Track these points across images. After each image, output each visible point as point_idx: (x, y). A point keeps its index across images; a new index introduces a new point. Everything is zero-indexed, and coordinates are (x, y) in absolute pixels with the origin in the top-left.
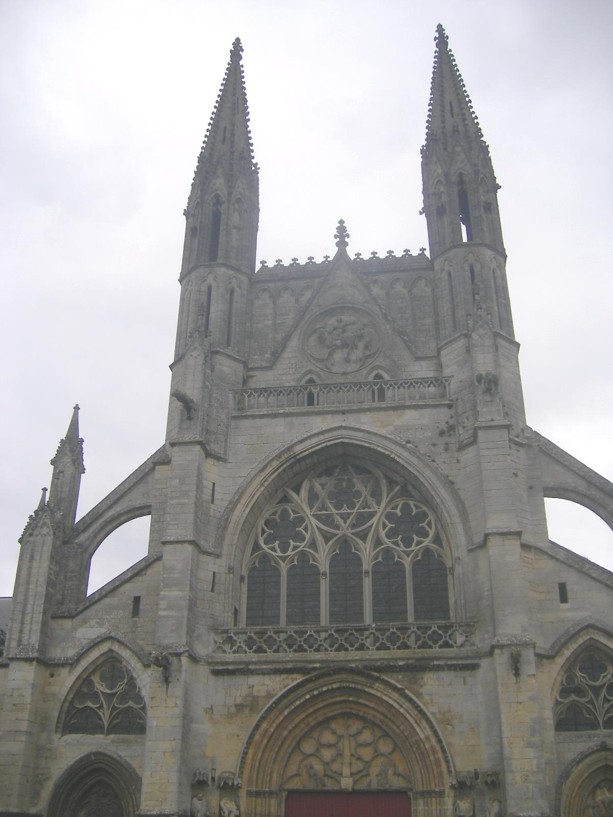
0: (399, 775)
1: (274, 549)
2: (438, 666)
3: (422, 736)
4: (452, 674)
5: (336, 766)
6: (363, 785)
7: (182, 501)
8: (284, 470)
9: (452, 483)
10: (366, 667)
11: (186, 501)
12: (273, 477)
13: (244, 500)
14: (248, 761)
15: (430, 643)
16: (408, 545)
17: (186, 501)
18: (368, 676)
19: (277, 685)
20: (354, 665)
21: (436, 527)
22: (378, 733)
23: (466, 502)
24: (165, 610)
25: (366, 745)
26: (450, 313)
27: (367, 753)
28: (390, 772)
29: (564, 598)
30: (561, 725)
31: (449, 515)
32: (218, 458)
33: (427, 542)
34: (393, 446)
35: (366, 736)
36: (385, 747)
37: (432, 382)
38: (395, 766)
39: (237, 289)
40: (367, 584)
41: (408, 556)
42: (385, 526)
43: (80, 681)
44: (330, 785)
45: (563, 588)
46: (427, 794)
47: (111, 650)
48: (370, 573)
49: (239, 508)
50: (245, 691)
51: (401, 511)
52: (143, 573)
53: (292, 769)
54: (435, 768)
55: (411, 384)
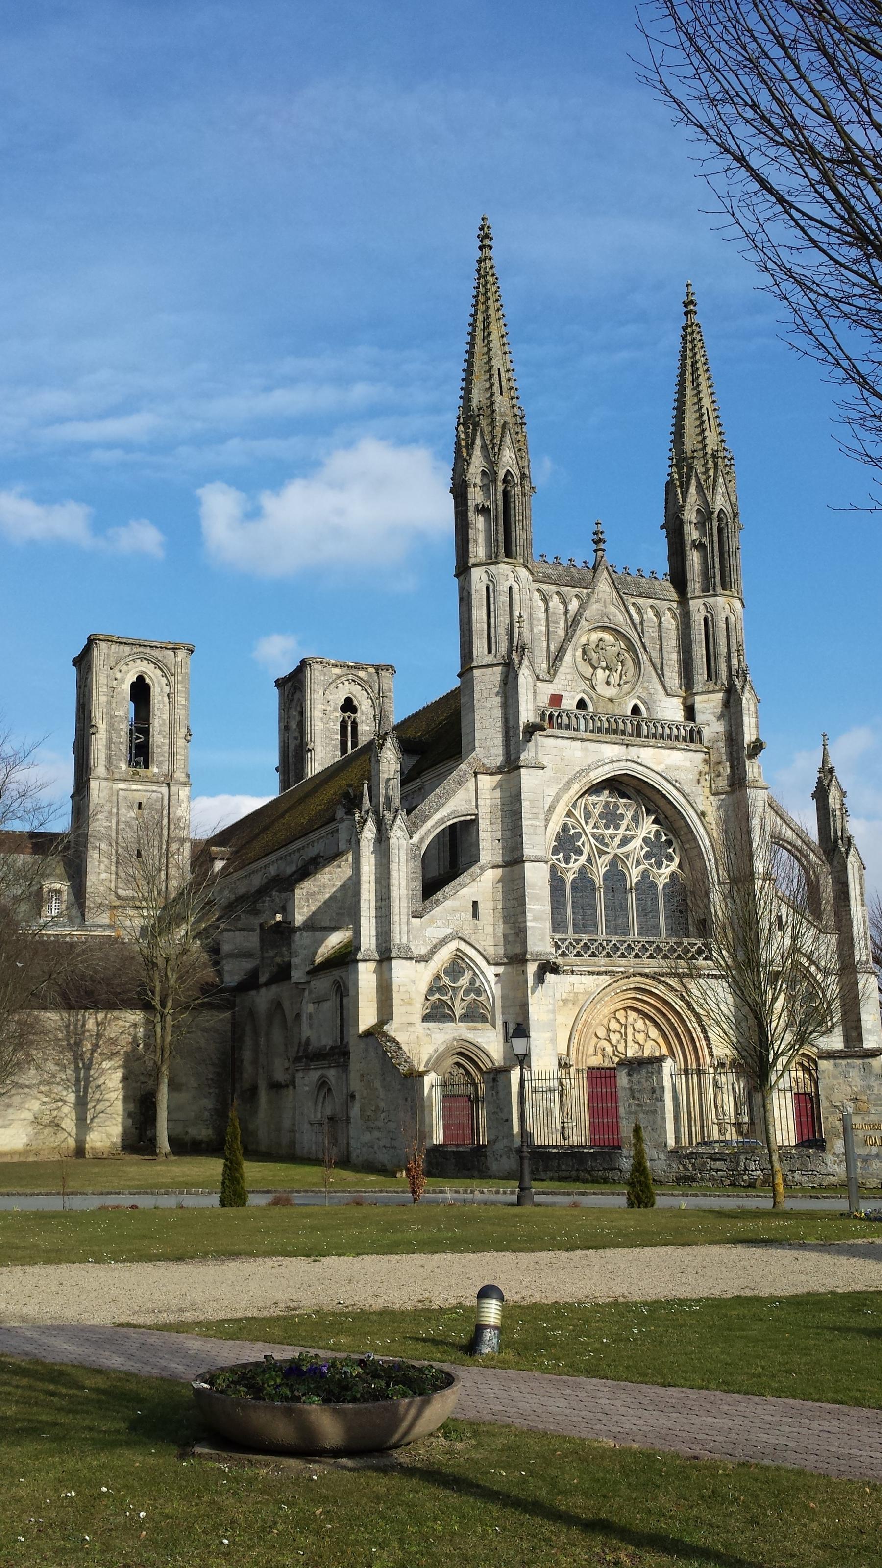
7: (534, 822)
10: (655, 973)
11: (538, 823)
42: (642, 848)
47: (458, 949)
50: (569, 989)
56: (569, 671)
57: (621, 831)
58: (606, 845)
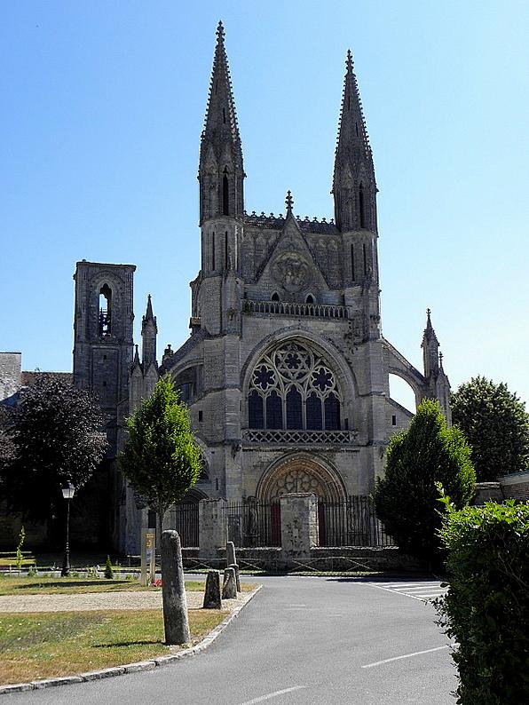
13: (252, 362)
16: (323, 390)
19: (270, 456)
33: (332, 389)
36: (314, 484)
40: (304, 407)
45: (394, 417)
57: (299, 370)
58: (289, 378)
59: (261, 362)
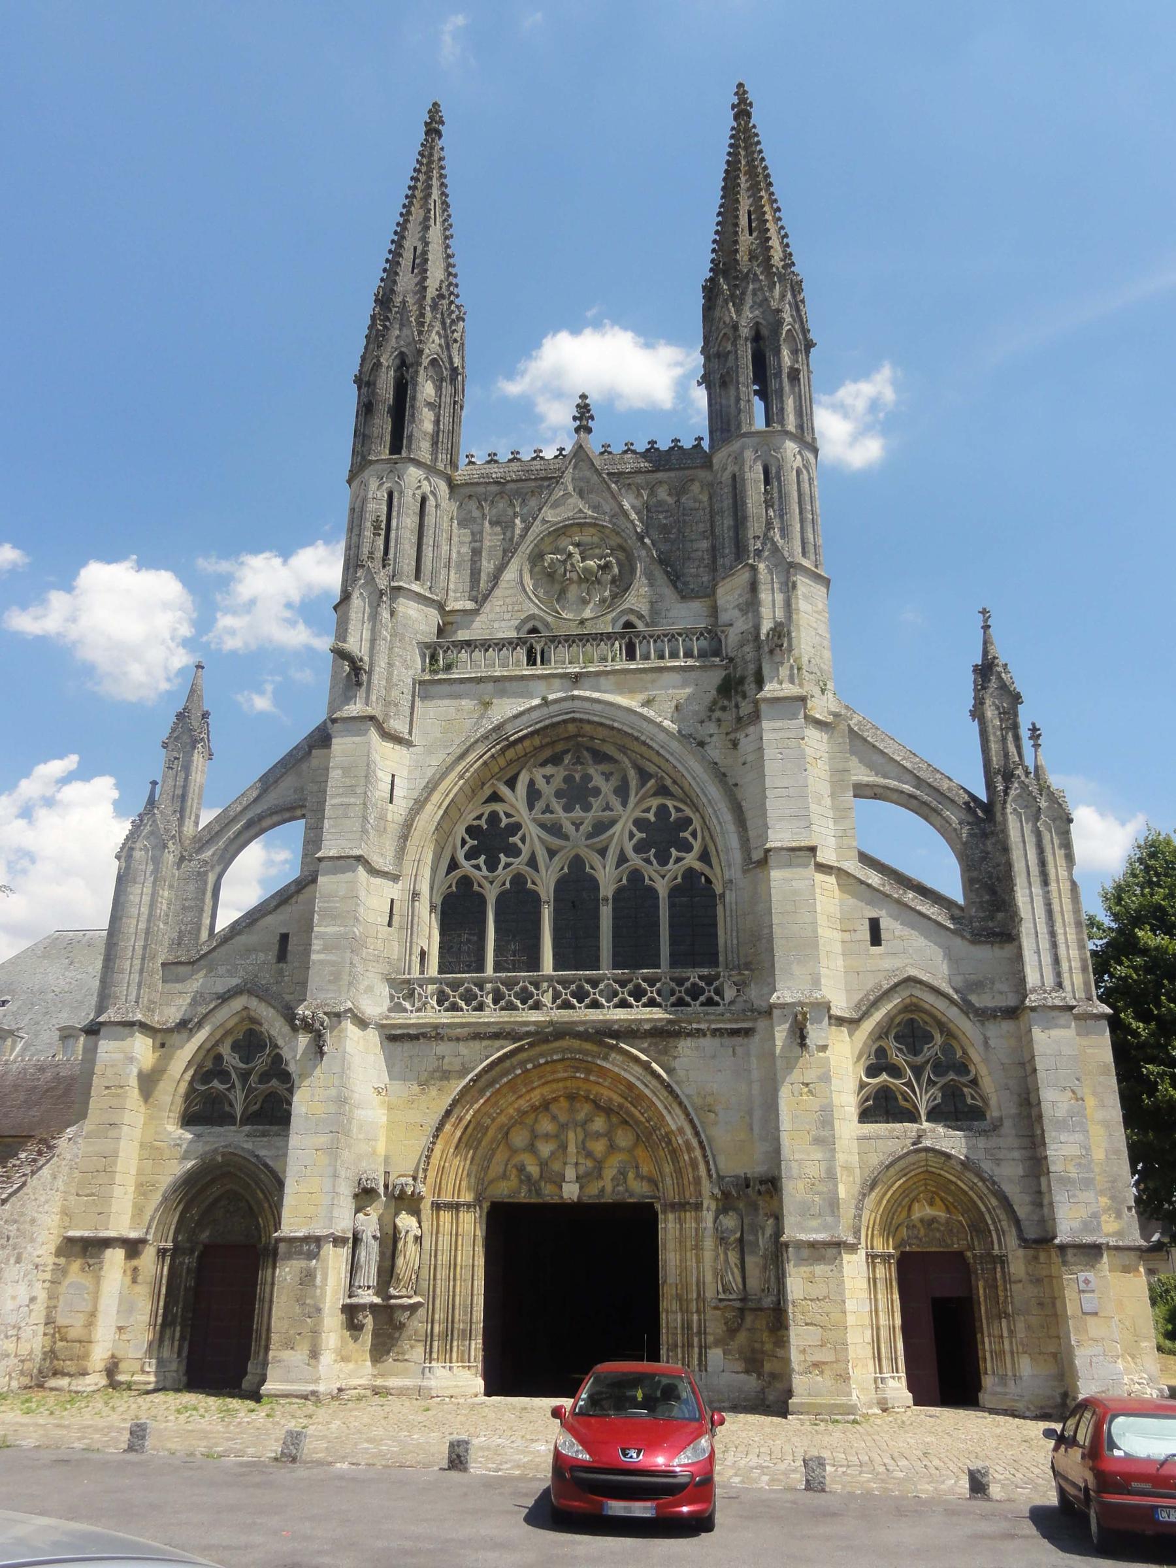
0: (642, 1178)
1: (478, 867)
2: (698, 1030)
3: (674, 1127)
4: (717, 1041)
5: (556, 1166)
6: (593, 1189)
7: (345, 800)
8: (493, 756)
9: (724, 775)
10: (598, 1032)
11: (352, 800)
12: (476, 766)
13: (436, 797)
14: (435, 1160)
15: (688, 999)
17: (352, 800)
18: (601, 1043)
20: (581, 1029)
21: (703, 838)
22: (614, 1120)
23: (743, 804)
24: (319, 952)
25: (598, 1136)
26: (731, 534)
27: (599, 1147)
28: (631, 1175)
29: (876, 939)
30: (866, 1116)
31: (720, 823)
32: (397, 740)
33: (691, 860)
34: (645, 725)
35: (599, 1124)
36: (624, 1139)
37: (701, 634)
38: (637, 1167)
39: (431, 498)
40: (606, 913)
41: (663, 877)
42: (632, 835)
43: (203, 1053)
44: (548, 1194)
45: (875, 925)
46: (680, 1207)
48: (610, 901)
49: (429, 808)
51: (656, 815)
52: (293, 900)
53: (496, 1169)
54: (690, 1170)
55: (673, 636)
56: (510, 592)
59: (489, 800)
